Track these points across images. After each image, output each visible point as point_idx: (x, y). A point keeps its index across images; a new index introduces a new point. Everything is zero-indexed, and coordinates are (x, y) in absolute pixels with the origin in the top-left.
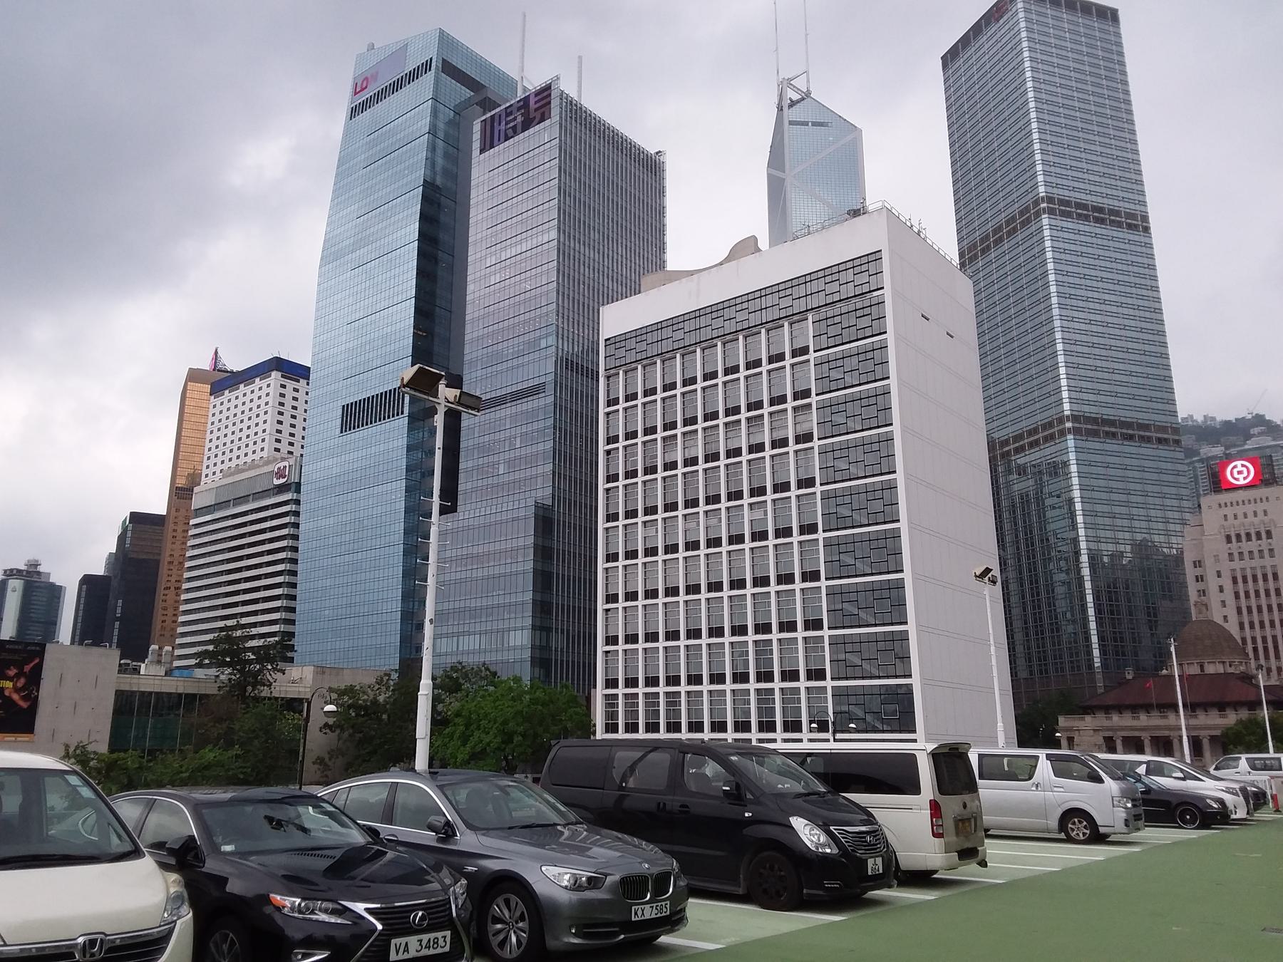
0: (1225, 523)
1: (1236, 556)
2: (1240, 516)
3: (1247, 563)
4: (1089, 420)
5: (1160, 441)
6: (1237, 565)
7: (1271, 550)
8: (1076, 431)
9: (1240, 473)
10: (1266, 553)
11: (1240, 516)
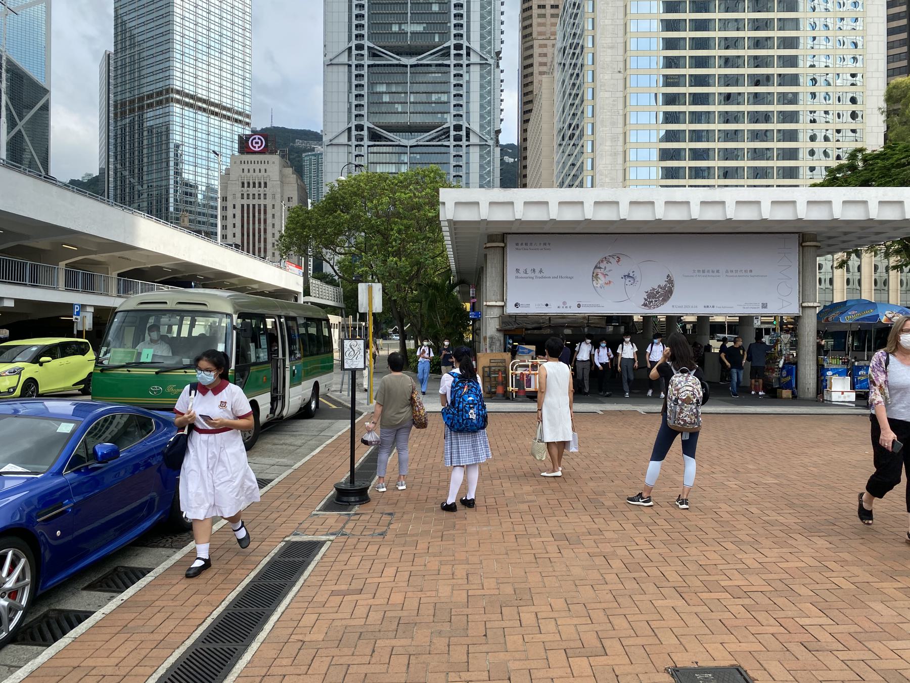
0: (243, 175)
1: (245, 196)
2: (252, 171)
3: (251, 202)
4: (187, 95)
5: (236, 121)
6: (245, 202)
7: (265, 195)
8: (178, 101)
9: (257, 143)
10: (262, 196)
11: (252, 171)
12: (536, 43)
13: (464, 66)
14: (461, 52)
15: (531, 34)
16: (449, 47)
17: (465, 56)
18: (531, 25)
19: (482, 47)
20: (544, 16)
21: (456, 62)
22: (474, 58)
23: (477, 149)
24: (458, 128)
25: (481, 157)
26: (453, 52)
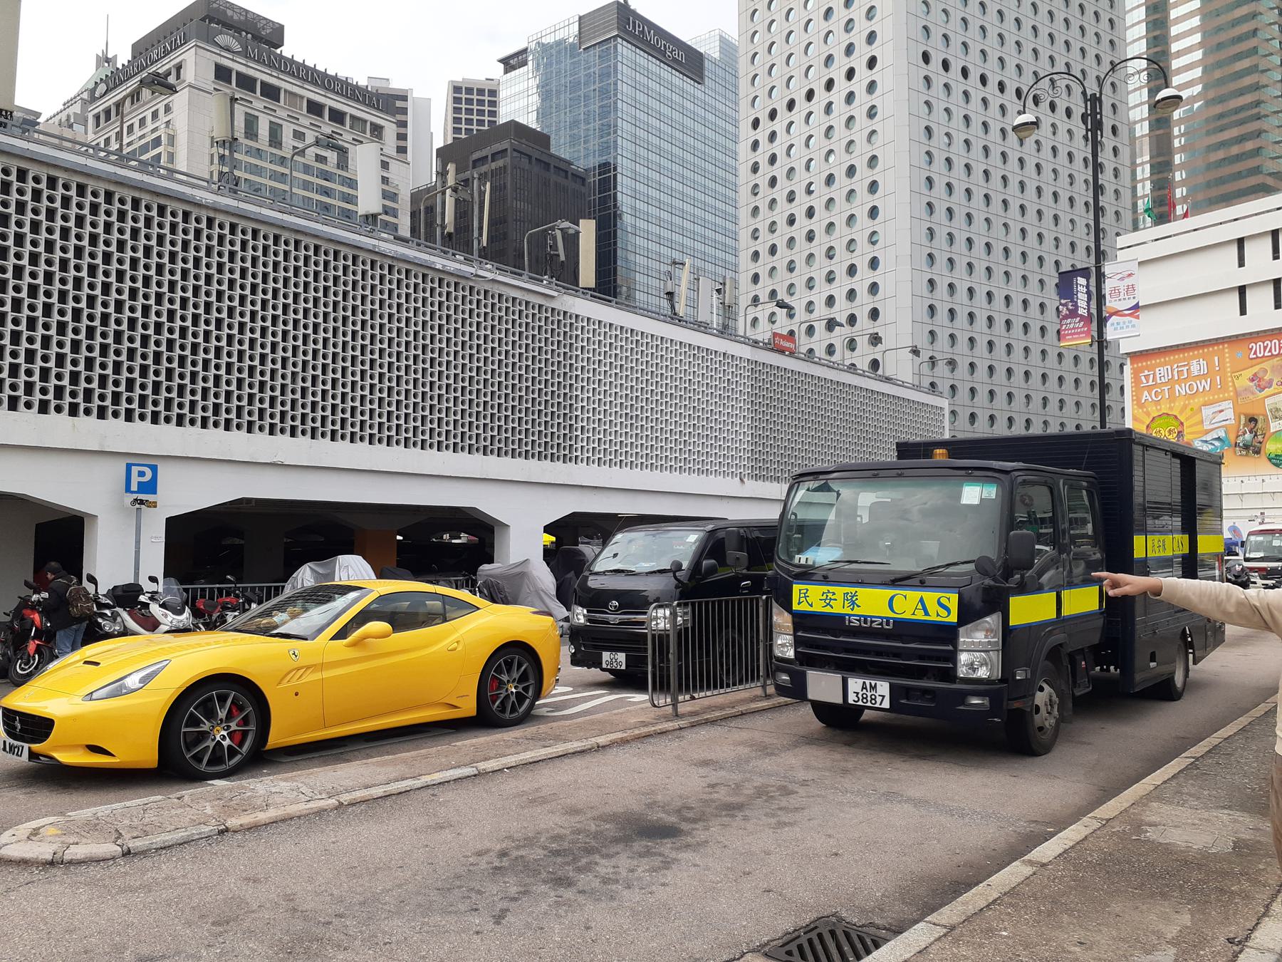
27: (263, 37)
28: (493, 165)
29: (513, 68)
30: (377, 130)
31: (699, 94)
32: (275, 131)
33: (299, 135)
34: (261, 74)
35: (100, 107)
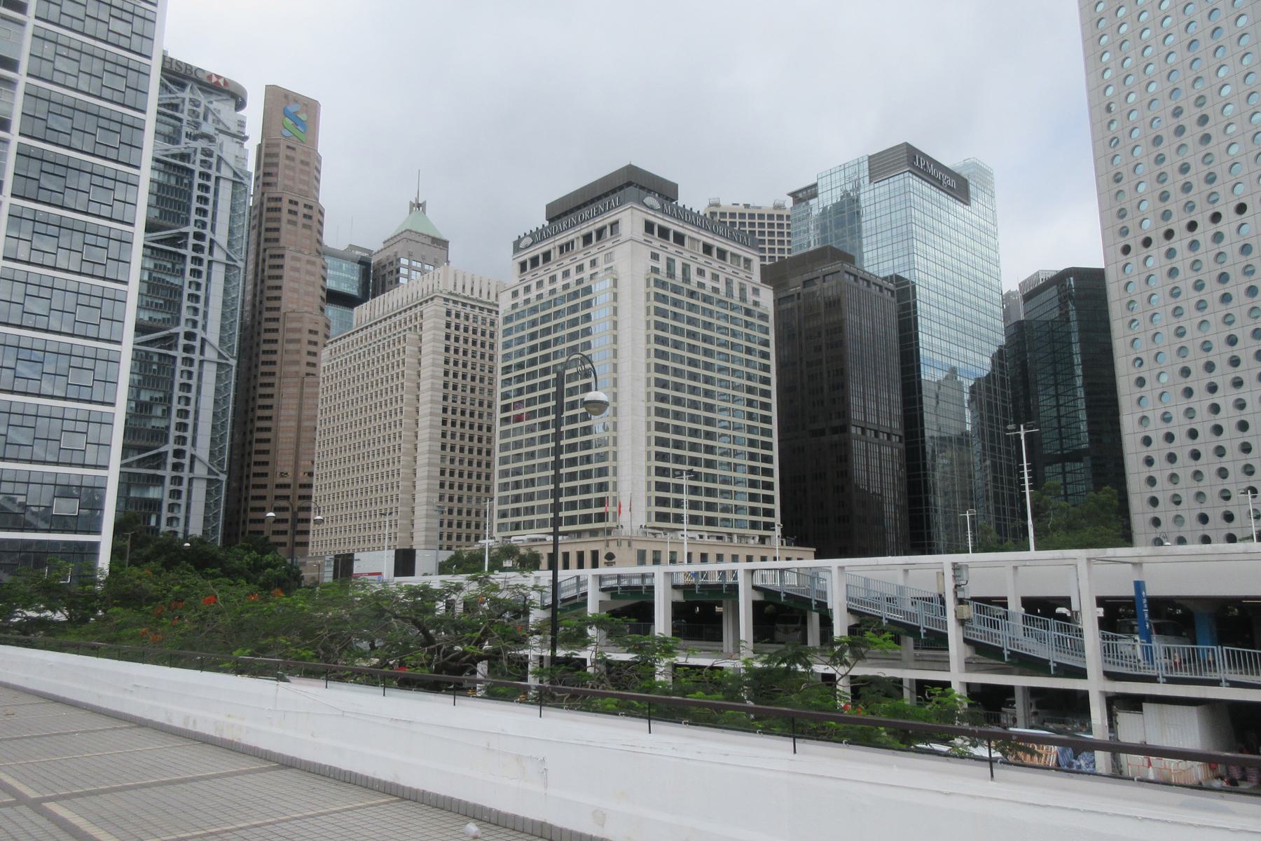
12: (288, 255)
13: (205, 263)
14: (202, 243)
15: (277, 240)
16: (186, 234)
17: (207, 250)
18: (277, 230)
19: (230, 244)
20: (294, 223)
21: (195, 254)
22: (219, 255)
23: (214, 367)
24: (190, 336)
25: (218, 377)
26: (192, 241)
27: (665, 192)
28: (826, 285)
29: (801, 200)
30: (748, 261)
31: (968, 214)
32: (686, 268)
33: (701, 272)
34: (673, 226)
35: (527, 256)
